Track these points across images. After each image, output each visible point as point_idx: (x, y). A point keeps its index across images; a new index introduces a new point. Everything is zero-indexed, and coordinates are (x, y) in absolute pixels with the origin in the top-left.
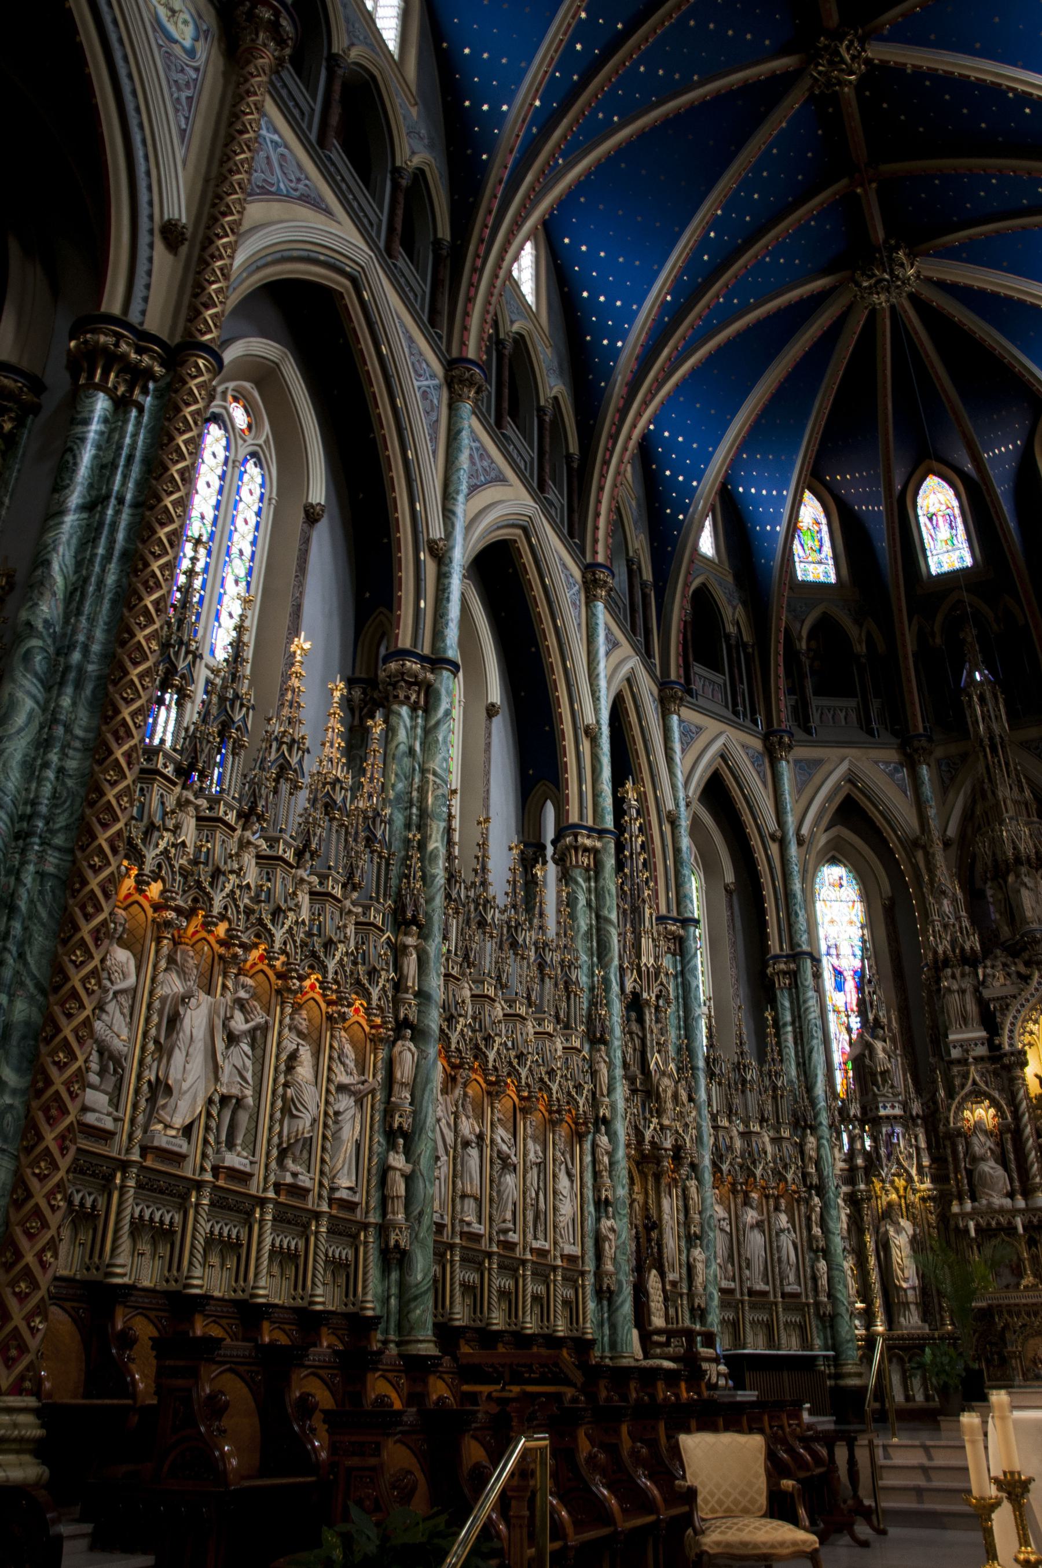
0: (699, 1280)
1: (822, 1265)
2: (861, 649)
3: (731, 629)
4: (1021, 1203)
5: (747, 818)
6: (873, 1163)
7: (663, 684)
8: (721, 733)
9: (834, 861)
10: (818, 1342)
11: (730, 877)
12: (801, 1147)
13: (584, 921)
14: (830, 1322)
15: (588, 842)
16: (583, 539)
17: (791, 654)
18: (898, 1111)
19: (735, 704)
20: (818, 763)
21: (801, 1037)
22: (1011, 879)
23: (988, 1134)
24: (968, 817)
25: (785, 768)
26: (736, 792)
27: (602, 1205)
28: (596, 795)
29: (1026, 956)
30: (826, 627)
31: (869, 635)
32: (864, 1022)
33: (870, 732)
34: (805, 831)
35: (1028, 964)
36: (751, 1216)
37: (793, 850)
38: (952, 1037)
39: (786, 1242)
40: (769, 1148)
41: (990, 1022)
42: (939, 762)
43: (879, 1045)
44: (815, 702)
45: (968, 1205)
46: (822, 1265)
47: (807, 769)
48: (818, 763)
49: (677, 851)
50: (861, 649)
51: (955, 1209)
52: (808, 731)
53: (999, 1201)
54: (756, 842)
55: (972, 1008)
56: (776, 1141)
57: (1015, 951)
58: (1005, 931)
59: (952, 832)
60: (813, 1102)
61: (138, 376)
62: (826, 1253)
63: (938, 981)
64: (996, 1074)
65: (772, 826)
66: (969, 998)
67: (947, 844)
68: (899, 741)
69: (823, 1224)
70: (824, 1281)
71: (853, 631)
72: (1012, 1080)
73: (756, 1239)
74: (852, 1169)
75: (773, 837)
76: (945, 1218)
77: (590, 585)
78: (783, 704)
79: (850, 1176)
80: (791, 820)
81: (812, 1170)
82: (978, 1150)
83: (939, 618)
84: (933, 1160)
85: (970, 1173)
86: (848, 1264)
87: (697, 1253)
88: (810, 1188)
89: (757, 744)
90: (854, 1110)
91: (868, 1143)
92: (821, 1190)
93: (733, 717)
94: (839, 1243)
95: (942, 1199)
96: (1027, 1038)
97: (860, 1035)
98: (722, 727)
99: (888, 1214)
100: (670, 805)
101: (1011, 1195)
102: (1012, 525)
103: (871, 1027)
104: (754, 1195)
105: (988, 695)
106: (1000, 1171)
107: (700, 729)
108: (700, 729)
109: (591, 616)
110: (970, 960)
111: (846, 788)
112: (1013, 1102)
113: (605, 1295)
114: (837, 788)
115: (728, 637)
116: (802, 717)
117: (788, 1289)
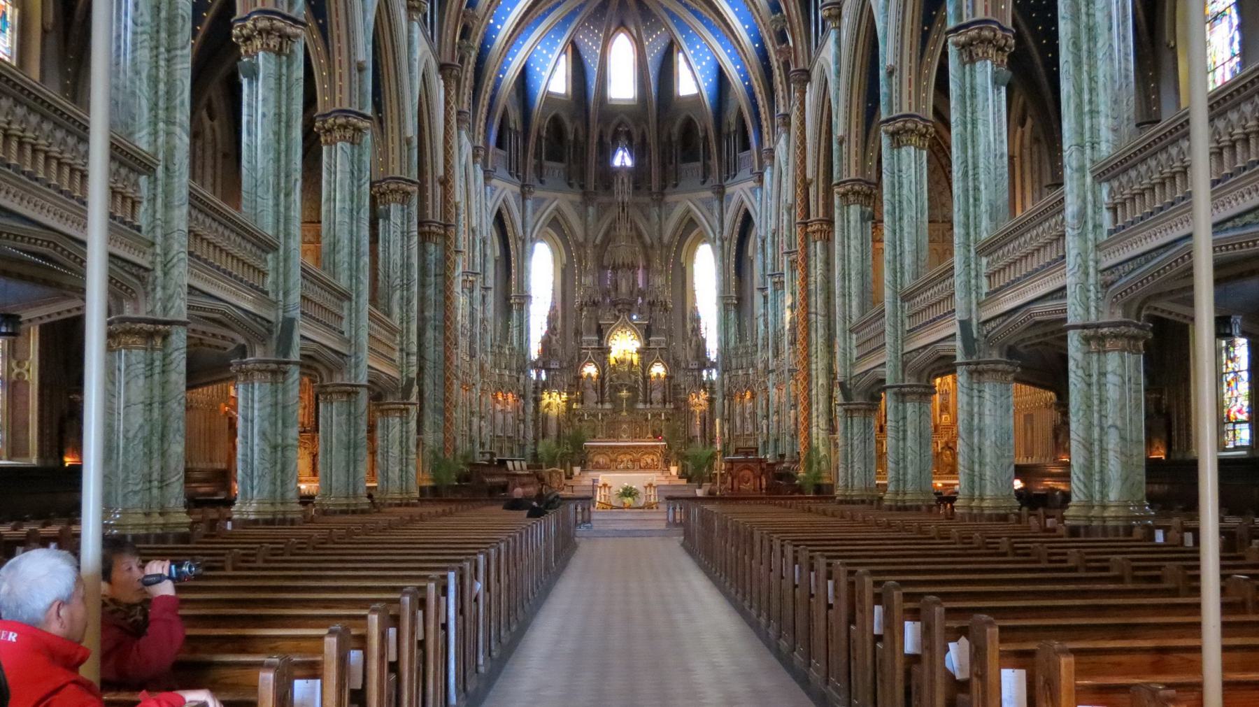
0: (483, 434)
1: (522, 426)
2: (571, 137)
3: (512, 125)
4: (600, 406)
5: (509, 229)
6: (546, 386)
7: (485, 172)
8: (504, 189)
9: (542, 241)
10: (517, 454)
11: (498, 253)
12: (518, 380)
13: (468, 309)
14: (522, 447)
15: (470, 278)
16: (474, 131)
17: (539, 137)
18: (558, 367)
19: (510, 169)
20: (543, 200)
21: (521, 333)
22: (619, 272)
23: (592, 378)
24: (607, 233)
25: (529, 203)
26: (506, 217)
27: (472, 413)
28: (473, 256)
29: (620, 307)
30: (556, 125)
31: (576, 130)
32: (549, 327)
33: (570, 185)
34: (534, 236)
35: (619, 311)
36: (499, 407)
37: (528, 246)
38: (584, 338)
39: (509, 417)
40: (507, 379)
41: (601, 332)
42: (599, 204)
43: (554, 338)
44: (547, 164)
45: (579, 406)
46: (522, 426)
47: (539, 202)
48: (543, 200)
49: (485, 255)
50: (571, 137)
51: (574, 406)
52: (542, 182)
53: (592, 405)
54: (511, 241)
55: (594, 327)
56: (510, 376)
57: (614, 304)
58: (613, 294)
59: (598, 241)
60: (525, 361)
61: (438, 234)
62: (524, 421)
63: (581, 310)
64: (599, 354)
65: (521, 233)
66: (593, 321)
67: (595, 246)
68: (581, 191)
69: (524, 410)
70: (522, 432)
71: (569, 127)
72: (605, 358)
73: (500, 417)
74: (537, 388)
75: (520, 238)
76: (569, 409)
77: (475, 156)
78: (531, 161)
79: (535, 392)
80: (529, 230)
81: (522, 389)
82: (587, 386)
83: (612, 127)
84: (569, 385)
85: (582, 393)
86: (530, 424)
87: (483, 423)
88: (520, 396)
89: (518, 189)
90: (540, 364)
91: (544, 376)
92: (524, 397)
93: (511, 179)
94: (529, 418)
95: (568, 402)
96: (613, 342)
97: (547, 332)
98: (507, 185)
99: (549, 405)
100: (485, 234)
101: (597, 403)
102: (654, 94)
103: (552, 330)
104: (500, 399)
105: (626, 180)
106: (595, 395)
107: (496, 187)
108: (496, 187)
109: (475, 171)
110: (595, 304)
111: (555, 213)
112: (604, 370)
113: (472, 441)
114: (551, 213)
115: (510, 129)
116: (539, 170)
117: (510, 435)
